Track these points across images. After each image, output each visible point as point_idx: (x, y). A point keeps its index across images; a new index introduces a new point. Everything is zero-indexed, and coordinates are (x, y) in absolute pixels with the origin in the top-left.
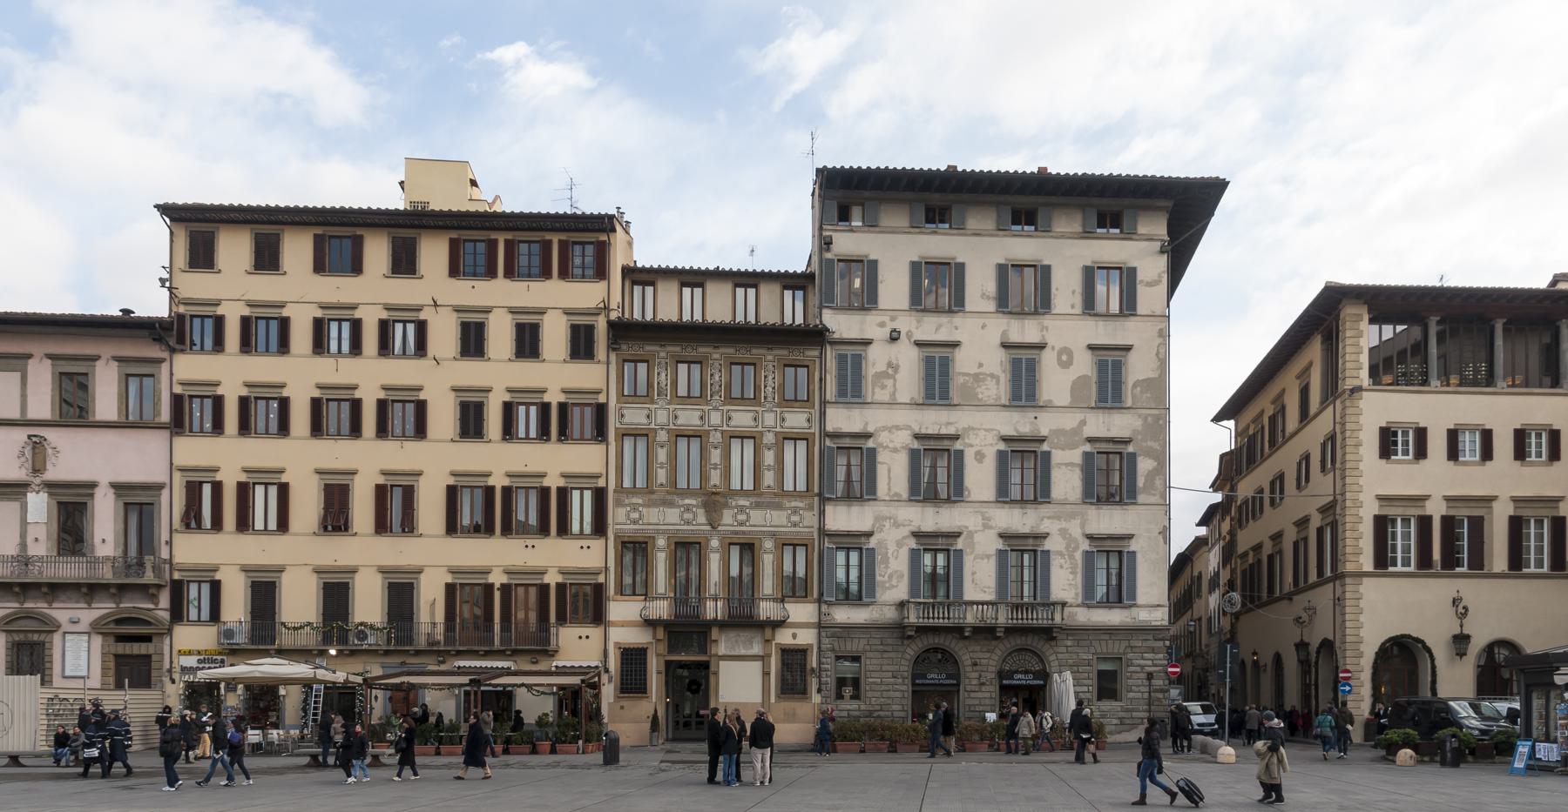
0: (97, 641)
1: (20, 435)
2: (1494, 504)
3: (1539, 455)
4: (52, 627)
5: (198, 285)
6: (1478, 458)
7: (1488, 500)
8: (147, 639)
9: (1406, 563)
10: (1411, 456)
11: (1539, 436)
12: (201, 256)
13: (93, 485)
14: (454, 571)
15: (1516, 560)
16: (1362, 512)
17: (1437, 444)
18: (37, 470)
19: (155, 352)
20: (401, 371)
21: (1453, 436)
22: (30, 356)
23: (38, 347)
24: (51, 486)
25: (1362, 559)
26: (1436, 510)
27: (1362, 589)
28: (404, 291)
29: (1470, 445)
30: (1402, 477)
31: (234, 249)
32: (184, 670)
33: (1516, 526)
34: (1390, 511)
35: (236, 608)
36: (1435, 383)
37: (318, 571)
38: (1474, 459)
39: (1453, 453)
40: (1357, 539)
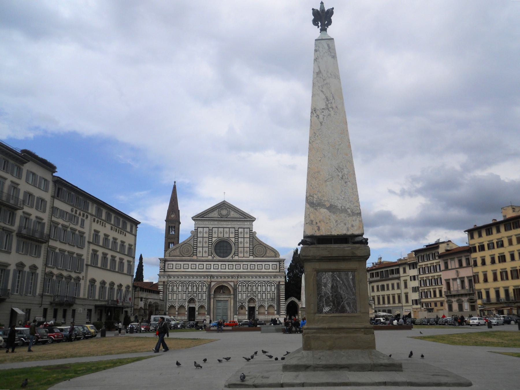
0: (468, 303)
1: (455, 270)
4: (463, 302)
5: (472, 242)
8: (474, 302)
12: (472, 237)
13: (464, 278)
14: (514, 286)
18: (458, 276)
19: (469, 254)
20: (501, 250)
22: (455, 258)
23: (455, 256)
24: (460, 278)
28: (499, 236)
31: (476, 235)
32: (479, 307)
35: (484, 296)
37: (495, 288)
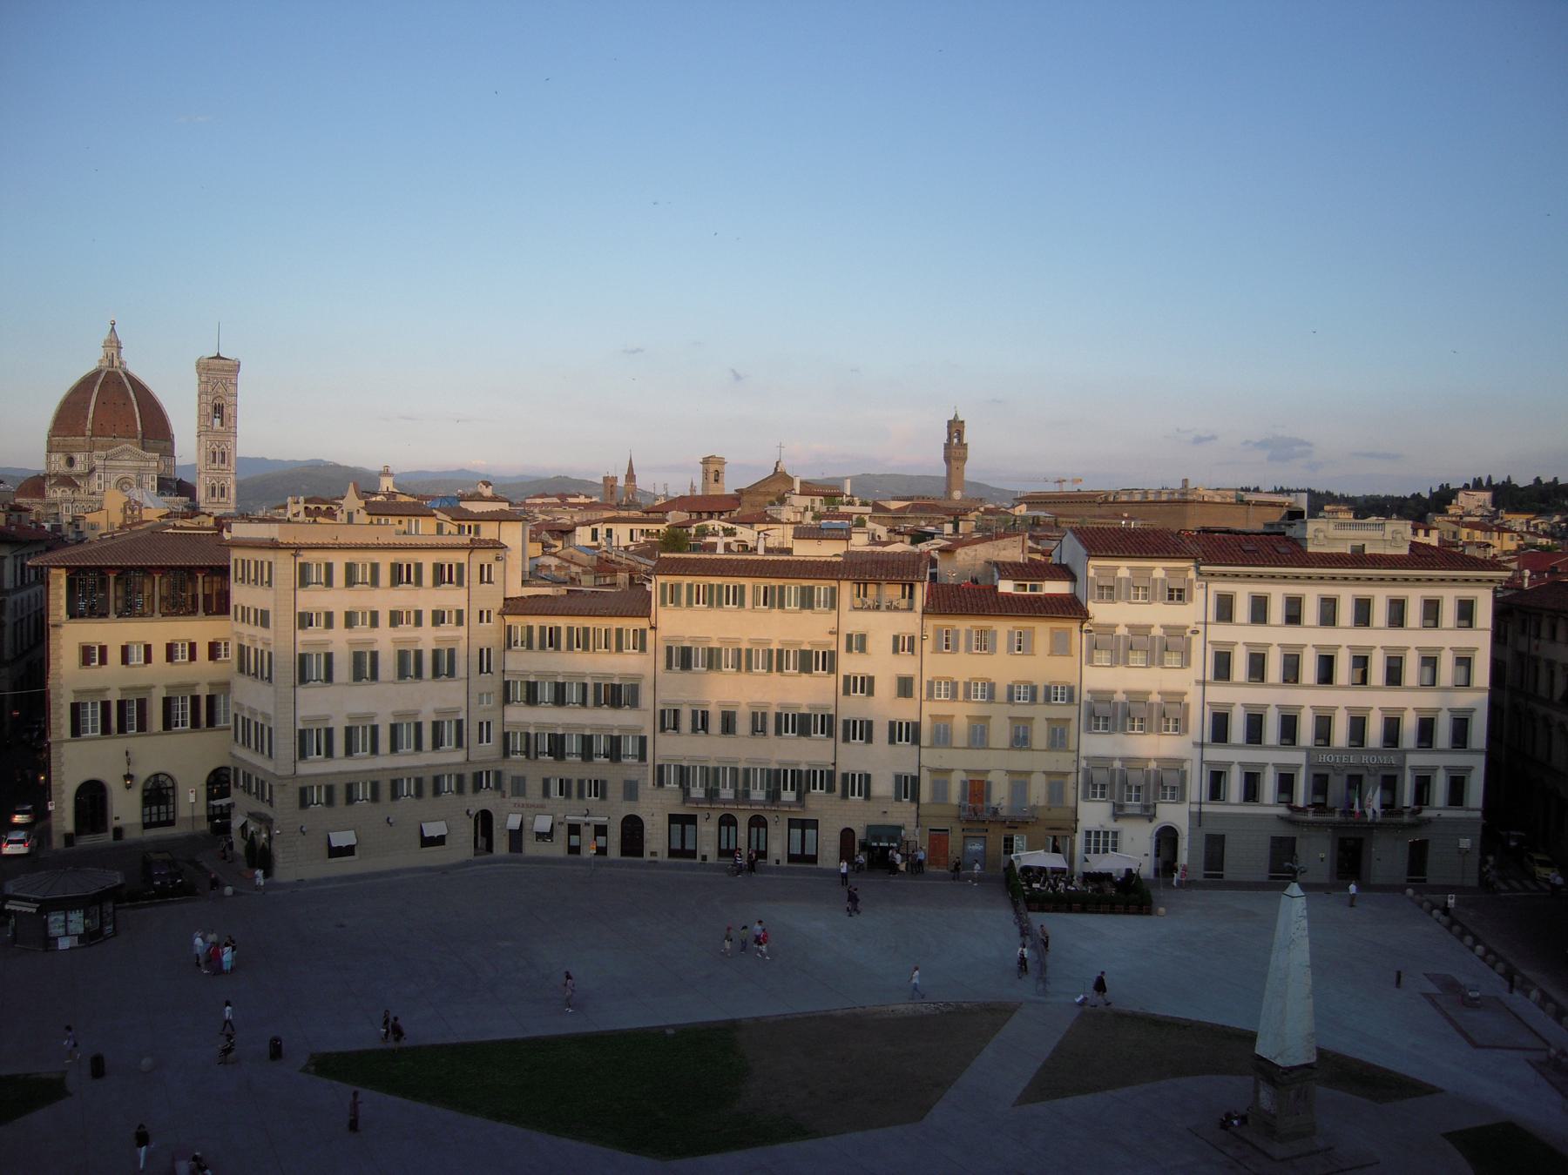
2: (153, 690)
3: (183, 657)
6: (142, 662)
7: (149, 688)
9: (94, 730)
10: (187, 659)
11: (183, 645)
15: (168, 724)
16: (62, 701)
17: (114, 655)
21: (125, 652)
25: (63, 731)
26: (114, 697)
27: (62, 750)
29: (137, 655)
30: (95, 677)
33: (167, 703)
34: (83, 700)
36: (112, 616)
38: (139, 663)
39: (125, 659)
40: (59, 719)
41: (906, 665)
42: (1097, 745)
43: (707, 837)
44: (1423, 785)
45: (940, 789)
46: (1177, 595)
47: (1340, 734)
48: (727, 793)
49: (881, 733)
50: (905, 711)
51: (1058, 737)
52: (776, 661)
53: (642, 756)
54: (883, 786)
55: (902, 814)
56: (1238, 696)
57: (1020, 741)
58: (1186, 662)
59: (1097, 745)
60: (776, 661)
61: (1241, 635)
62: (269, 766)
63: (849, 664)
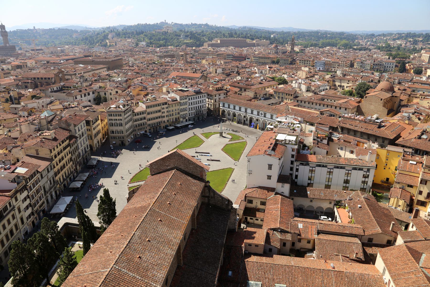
41: (167, 110)
42: (181, 113)
43: (152, 130)
44: (203, 111)
45: (170, 120)
46: (186, 99)
47: (197, 109)
48: (153, 126)
49: (165, 116)
50: (167, 114)
51: (179, 113)
52: (157, 112)
53: (146, 124)
54: (166, 121)
55: (168, 124)
56: (190, 107)
57: (176, 115)
58: (187, 105)
59: (181, 113)
60: (157, 112)
61: (190, 101)
62: (123, 135)
63: (163, 111)
